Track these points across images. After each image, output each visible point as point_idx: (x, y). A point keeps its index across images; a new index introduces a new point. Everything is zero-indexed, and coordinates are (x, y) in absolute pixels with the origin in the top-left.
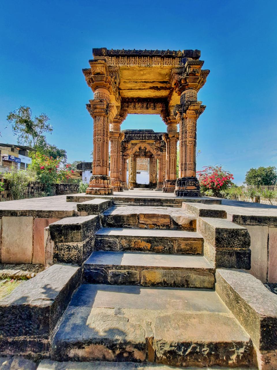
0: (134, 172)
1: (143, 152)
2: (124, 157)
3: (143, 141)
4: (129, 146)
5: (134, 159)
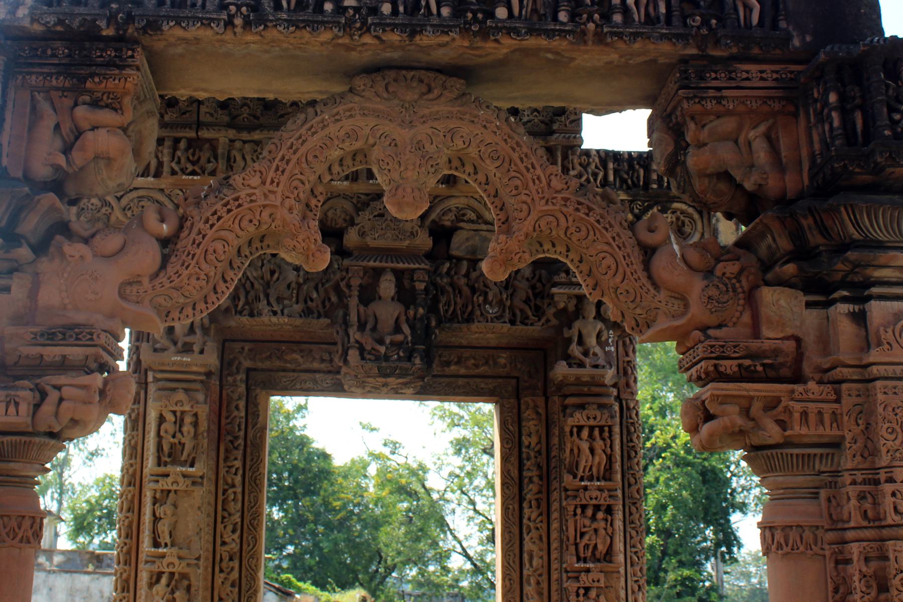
1: (387, 286)
4: (104, 141)
5: (221, 408)
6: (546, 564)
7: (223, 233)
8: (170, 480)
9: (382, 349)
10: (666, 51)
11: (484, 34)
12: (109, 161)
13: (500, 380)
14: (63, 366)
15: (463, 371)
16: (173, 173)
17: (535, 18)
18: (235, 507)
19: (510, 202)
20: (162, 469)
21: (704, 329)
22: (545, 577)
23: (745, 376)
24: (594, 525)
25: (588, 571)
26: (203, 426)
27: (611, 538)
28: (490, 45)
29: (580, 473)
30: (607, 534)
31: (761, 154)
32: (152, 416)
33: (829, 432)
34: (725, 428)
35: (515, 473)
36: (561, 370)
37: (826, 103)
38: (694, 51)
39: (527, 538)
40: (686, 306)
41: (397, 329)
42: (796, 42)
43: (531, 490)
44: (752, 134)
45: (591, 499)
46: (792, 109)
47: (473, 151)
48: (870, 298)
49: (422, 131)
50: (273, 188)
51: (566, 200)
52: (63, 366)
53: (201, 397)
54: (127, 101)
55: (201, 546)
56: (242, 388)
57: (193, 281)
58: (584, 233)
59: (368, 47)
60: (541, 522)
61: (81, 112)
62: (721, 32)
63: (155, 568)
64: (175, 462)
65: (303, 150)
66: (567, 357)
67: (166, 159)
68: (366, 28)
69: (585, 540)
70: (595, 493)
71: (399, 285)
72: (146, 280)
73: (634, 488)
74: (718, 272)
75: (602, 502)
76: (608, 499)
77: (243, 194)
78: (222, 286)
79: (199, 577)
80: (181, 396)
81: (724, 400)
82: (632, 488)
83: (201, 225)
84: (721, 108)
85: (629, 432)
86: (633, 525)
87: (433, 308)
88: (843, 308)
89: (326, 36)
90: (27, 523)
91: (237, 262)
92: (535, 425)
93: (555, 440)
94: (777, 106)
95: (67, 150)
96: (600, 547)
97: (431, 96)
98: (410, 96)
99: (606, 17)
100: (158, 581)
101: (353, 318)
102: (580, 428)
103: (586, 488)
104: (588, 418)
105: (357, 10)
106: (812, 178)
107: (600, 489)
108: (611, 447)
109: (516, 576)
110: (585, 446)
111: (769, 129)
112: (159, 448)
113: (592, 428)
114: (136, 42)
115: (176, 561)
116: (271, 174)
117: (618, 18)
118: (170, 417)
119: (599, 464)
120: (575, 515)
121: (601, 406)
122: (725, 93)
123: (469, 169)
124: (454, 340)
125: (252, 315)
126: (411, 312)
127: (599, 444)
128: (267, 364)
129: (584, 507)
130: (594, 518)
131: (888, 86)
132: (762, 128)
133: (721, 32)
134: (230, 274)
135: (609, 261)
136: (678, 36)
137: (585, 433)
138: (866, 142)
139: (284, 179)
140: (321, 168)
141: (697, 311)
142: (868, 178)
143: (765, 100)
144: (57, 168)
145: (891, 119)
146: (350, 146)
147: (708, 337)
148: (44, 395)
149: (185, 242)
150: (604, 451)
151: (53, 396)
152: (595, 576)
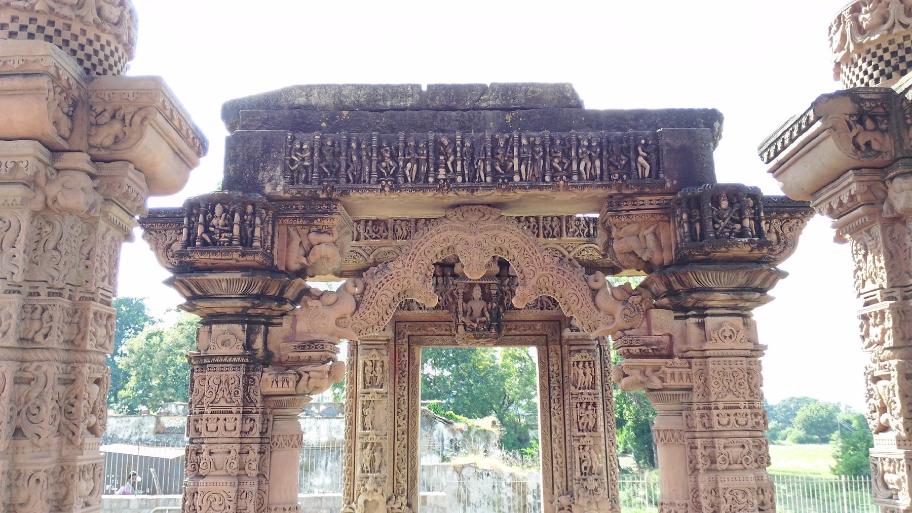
0: (395, 494)
1: (477, 293)
2: (268, 382)
3: (481, 195)
7: (385, 292)
8: (370, 395)
9: (475, 325)
10: (601, 192)
11: (509, 189)
12: (328, 258)
14: (310, 361)
15: (518, 333)
16: (366, 238)
17: (534, 179)
18: (404, 407)
19: (525, 270)
20: (366, 390)
21: (623, 330)
23: (643, 355)
24: (587, 413)
25: (584, 436)
26: (386, 366)
28: (511, 194)
29: (579, 386)
31: (651, 242)
32: (361, 363)
33: (685, 383)
34: (633, 382)
35: (546, 384)
36: (567, 333)
37: (682, 219)
38: (616, 192)
39: (553, 418)
40: (614, 319)
41: (483, 315)
42: (668, 185)
43: (555, 394)
44: (646, 232)
46: (666, 218)
47: (506, 245)
48: (707, 315)
49: (481, 236)
50: (409, 268)
51: (552, 268)
52: (310, 361)
53: (385, 352)
54: (334, 229)
55: (388, 428)
56: (406, 346)
57: (372, 315)
58: (561, 284)
59: (451, 197)
61: (312, 236)
62: (628, 182)
63: (364, 441)
64: (372, 387)
65: (422, 249)
66: (570, 326)
67: (362, 231)
68: (450, 189)
71: (483, 292)
72: (348, 316)
73: (608, 392)
74: (630, 301)
77: (394, 272)
78: (386, 317)
79: (387, 445)
80: (374, 352)
81: (632, 368)
83: (374, 288)
84: (628, 220)
87: (501, 303)
88: (693, 320)
89: (430, 194)
90: (295, 438)
91: (393, 305)
93: (566, 368)
94: (658, 218)
95: (306, 255)
97: (485, 218)
98: (475, 219)
99: (569, 177)
100: (366, 447)
101: (460, 309)
102: (578, 362)
103: (582, 394)
105: (445, 180)
106: (676, 255)
109: (548, 438)
110: (581, 372)
111: (655, 229)
112: (365, 379)
113: (584, 362)
114: (338, 200)
115: (375, 437)
116: (407, 262)
117: (575, 178)
118: (369, 364)
121: (589, 351)
122: (631, 212)
123: (505, 253)
124: (513, 318)
125: (409, 310)
126: (490, 306)
127: (588, 371)
128: (418, 333)
129: (581, 403)
130: (586, 408)
131: (713, 210)
132: (651, 229)
133: (628, 182)
134: (389, 311)
135: (574, 298)
136: (606, 186)
137: (581, 365)
138: (702, 239)
139: (413, 264)
140: (432, 256)
141: (620, 321)
142: (704, 257)
143: (653, 215)
144: (302, 264)
145: (714, 228)
146: (445, 245)
147: (625, 335)
148: (301, 376)
149: (367, 297)
151: (305, 376)
152: (588, 439)
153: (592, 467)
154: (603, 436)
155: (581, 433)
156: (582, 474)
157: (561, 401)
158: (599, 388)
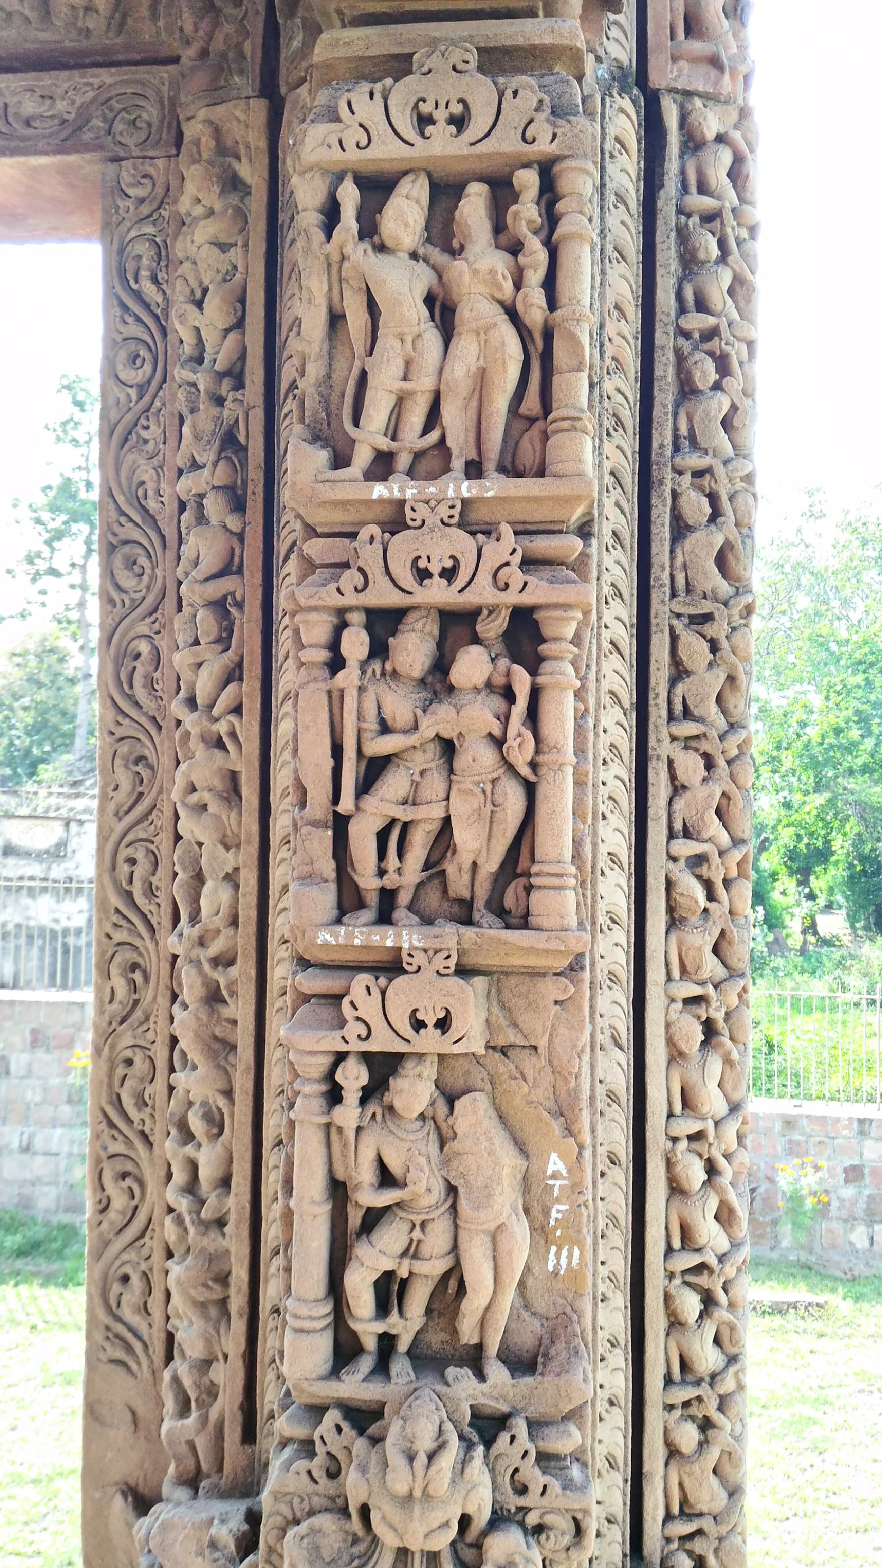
6: (248, 913)
13: (106, 76)
22: (243, 971)
24: (442, 720)
25: (392, 966)
27: (530, 789)
30: (510, 768)
45: (423, 575)
60: (237, 710)
69: (387, 799)
70: (444, 546)
73: (703, 545)
75: (482, 593)
76: (515, 575)
82: (689, 543)
85: (690, 261)
86: (689, 728)
92: (223, 247)
96: (467, 838)
103: (396, 521)
104: (424, 121)
107: (471, 521)
108: (550, 284)
110: (403, 286)
119: (482, 381)
120: (336, 663)
127: (480, 270)
129: (384, 624)
130: (438, 681)
137: (406, 213)
150: (512, 313)
152: (431, 996)
153: (451, 1287)
154: (613, 951)
155: (362, 935)
156: (346, 1350)
157: (248, 625)
158: (593, 458)
